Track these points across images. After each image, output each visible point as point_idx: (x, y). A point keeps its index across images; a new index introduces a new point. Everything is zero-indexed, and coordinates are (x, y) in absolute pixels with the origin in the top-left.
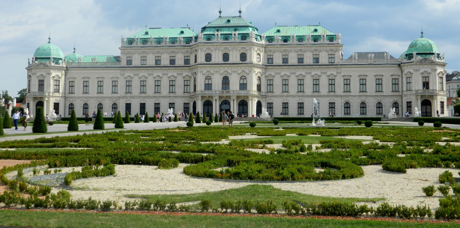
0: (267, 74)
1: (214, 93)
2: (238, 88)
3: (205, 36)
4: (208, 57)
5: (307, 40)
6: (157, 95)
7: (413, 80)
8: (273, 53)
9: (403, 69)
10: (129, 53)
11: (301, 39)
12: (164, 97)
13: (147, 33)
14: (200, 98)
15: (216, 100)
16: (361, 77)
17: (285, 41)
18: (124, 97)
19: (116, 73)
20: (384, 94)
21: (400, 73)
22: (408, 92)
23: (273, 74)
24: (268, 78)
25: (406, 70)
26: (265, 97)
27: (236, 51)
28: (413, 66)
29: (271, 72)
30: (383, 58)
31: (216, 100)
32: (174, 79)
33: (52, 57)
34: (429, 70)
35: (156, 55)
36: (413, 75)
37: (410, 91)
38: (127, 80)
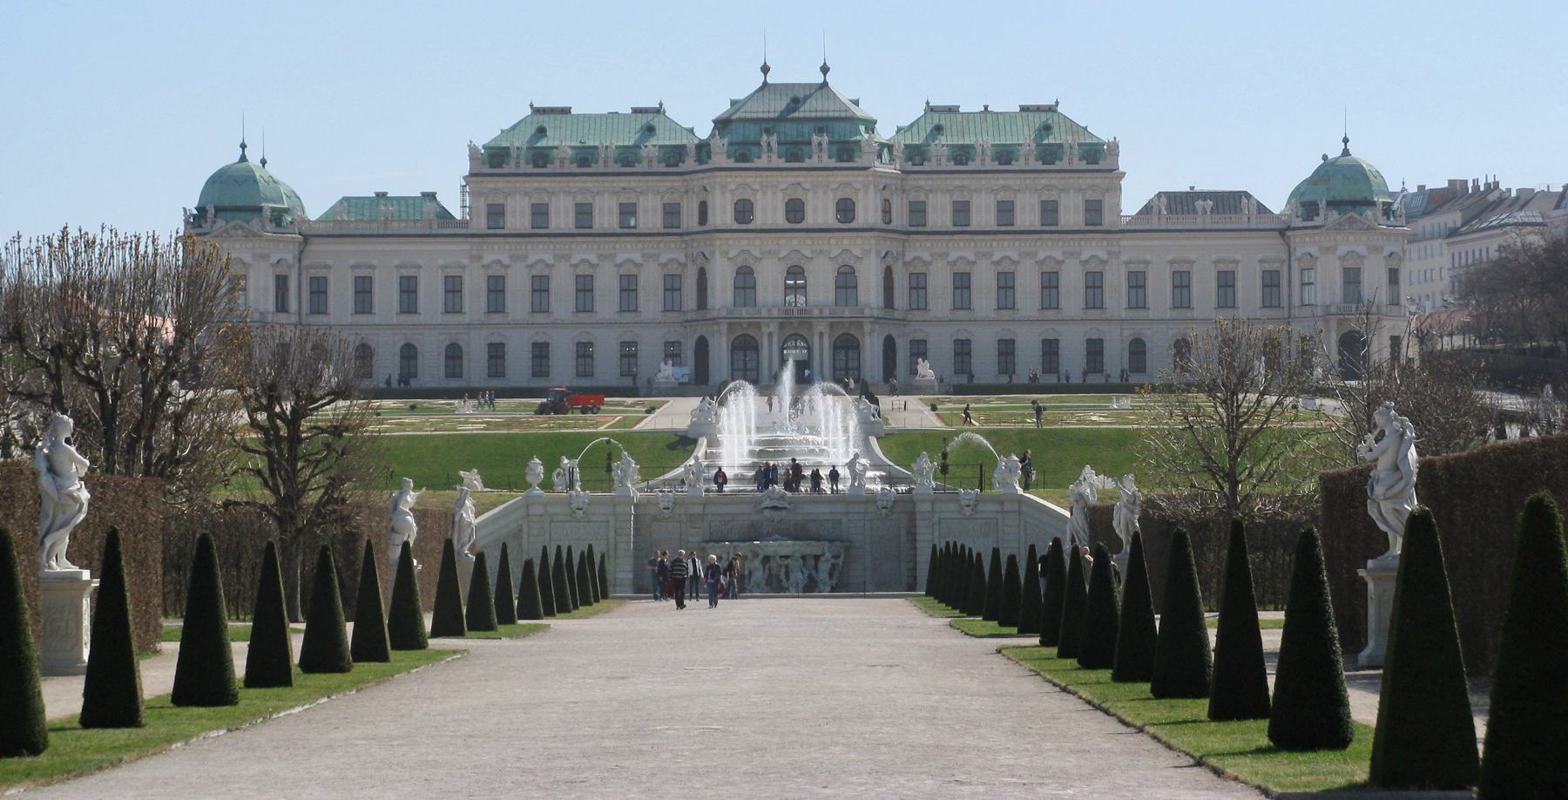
0: (909, 257)
1: (764, 313)
2: (831, 297)
3: (733, 149)
4: (744, 211)
5: (1022, 160)
6: (584, 317)
10: (496, 191)
11: (1005, 155)
13: (542, 131)
14: (724, 328)
15: (770, 334)
16: (1177, 267)
17: (958, 161)
21: (1284, 256)
23: (926, 256)
24: (911, 269)
26: (904, 321)
27: (825, 193)
29: (920, 250)
30: (1237, 210)
31: (770, 334)
32: (634, 271)
33: (267, 205)
34: (1361, 250)
35: (579, 199)
38: (490, 272)
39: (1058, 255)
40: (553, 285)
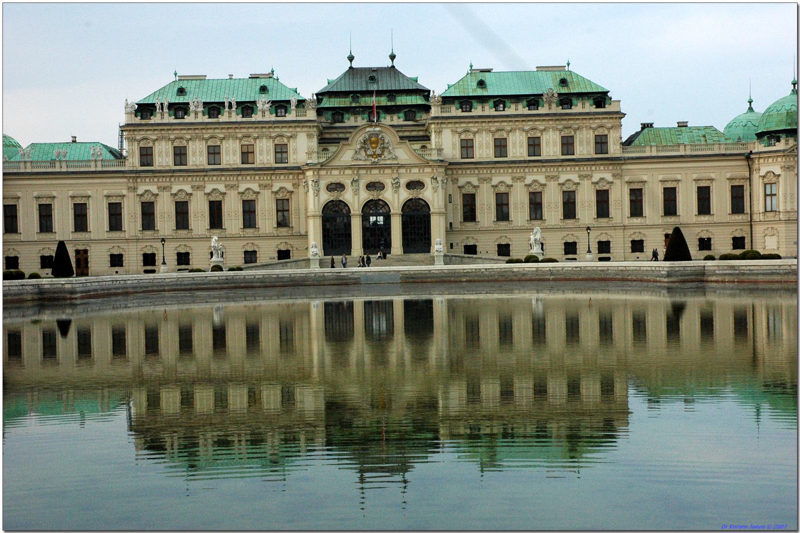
7: (781, 189)
8: (475, 133)
9: (756, 166)
11: (533, 101)
12: (233, 238)
13: (181, 91)
18: (138, 240)
19: (118, 187)
20: (715, 219)
22: (768, 214)
23: (475, 182)
25: (764, 167)
28: (779, 159)
35: (210, 143)
36: (781, 179)
37: (772, 214)
38: (144, 199)
39: (577, 180)
40: (192, 208)
